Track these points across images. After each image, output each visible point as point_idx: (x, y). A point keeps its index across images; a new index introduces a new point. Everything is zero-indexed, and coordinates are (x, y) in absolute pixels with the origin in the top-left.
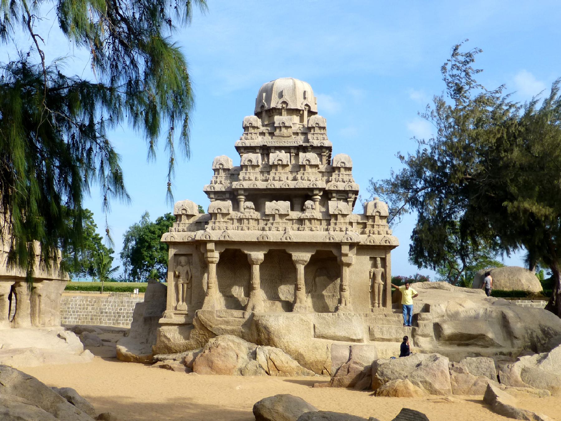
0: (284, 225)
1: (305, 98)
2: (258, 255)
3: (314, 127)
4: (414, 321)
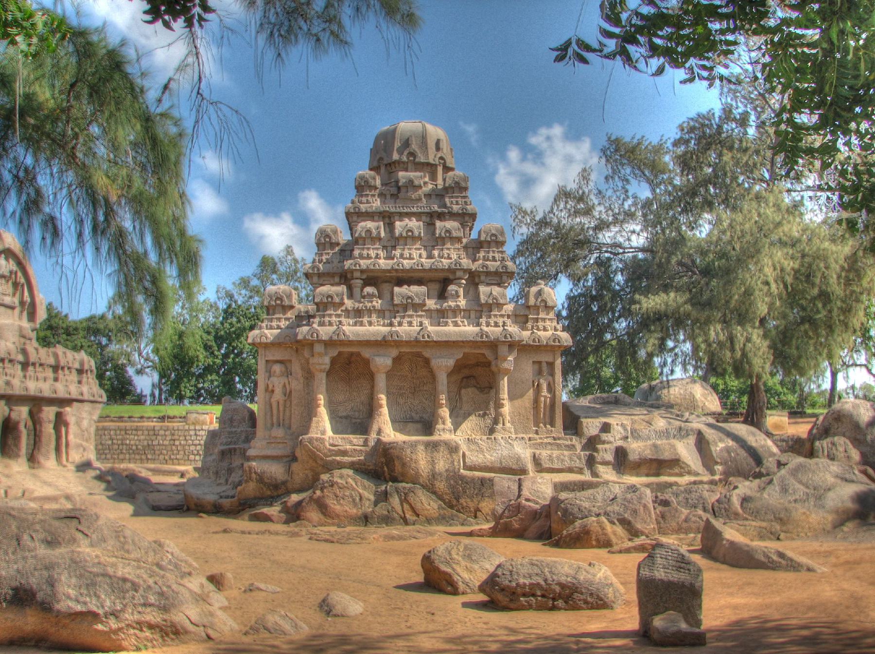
0: (419, 319)
3: (453, 188)
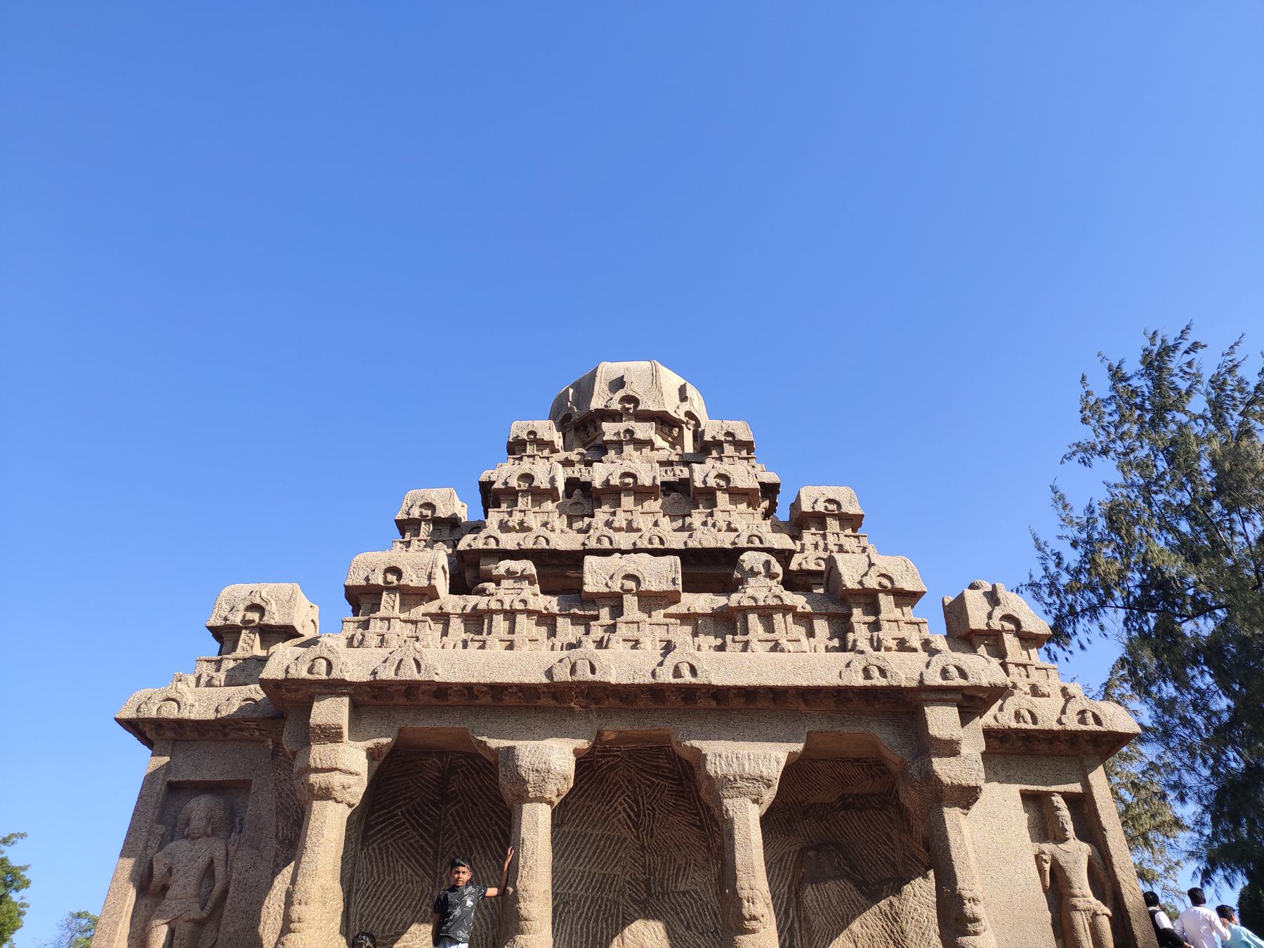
2: (552, 758)
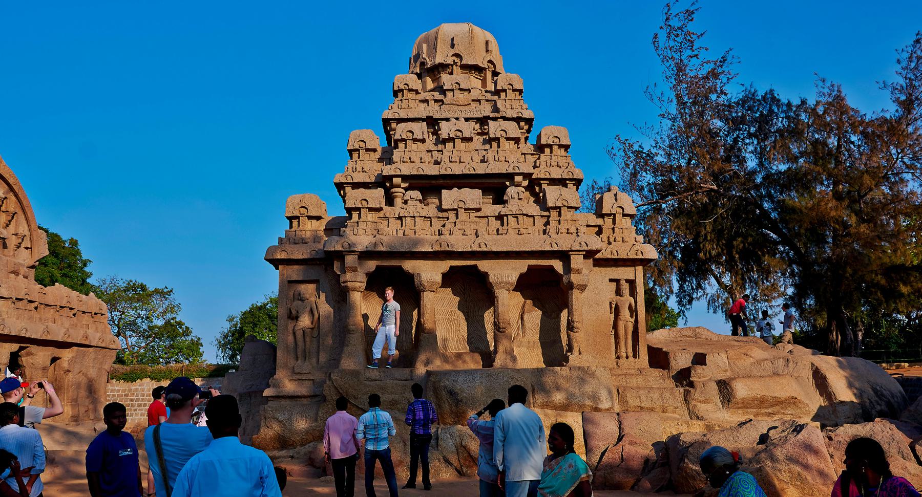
0: (473, 226)
1: (487, 51)
4: (683, 378)
